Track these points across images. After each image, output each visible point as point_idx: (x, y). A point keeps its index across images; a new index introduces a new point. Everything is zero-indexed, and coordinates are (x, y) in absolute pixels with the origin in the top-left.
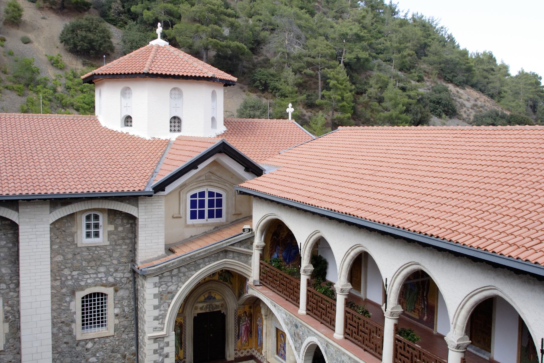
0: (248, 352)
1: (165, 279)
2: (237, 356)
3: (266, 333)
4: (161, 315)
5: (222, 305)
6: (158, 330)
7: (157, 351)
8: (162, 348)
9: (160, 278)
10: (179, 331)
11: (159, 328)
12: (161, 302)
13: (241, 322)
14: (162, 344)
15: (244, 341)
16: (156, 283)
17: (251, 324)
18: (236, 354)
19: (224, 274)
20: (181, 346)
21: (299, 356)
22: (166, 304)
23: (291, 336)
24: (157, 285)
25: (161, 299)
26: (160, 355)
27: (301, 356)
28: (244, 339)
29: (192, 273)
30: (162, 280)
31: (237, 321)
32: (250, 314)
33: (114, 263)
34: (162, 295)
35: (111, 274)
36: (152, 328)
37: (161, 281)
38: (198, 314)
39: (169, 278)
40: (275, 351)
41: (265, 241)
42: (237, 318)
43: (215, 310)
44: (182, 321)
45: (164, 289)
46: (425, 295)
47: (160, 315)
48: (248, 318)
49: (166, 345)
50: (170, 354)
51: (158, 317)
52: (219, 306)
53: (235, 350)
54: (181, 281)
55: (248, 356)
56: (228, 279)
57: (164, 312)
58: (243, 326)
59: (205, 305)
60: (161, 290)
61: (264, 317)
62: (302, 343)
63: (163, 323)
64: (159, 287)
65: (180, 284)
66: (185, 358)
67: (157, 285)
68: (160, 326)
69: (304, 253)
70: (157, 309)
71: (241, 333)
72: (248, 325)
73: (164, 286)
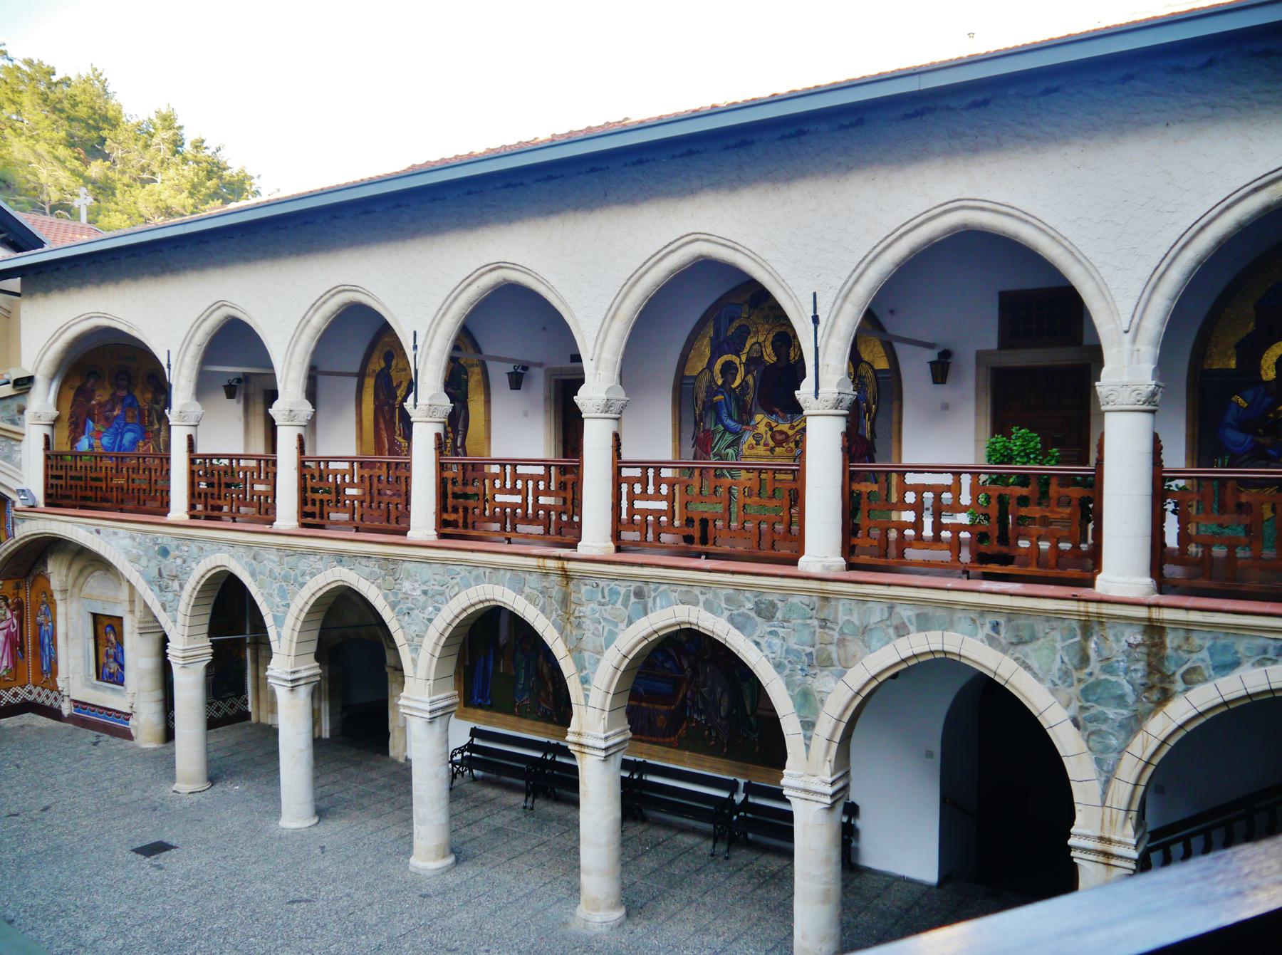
3: (67, 635)
21: (175, 621)
23: (149, 582)
27: (180, 618)
32: (18, 602)
40: (93, 671)
41: (58, 404)
46: (459, 444)
48: (12, 611)
55: (16, 705)
61: (57, 596)
62: (181, 587)
69: (179, 373)
72: (13, 630)
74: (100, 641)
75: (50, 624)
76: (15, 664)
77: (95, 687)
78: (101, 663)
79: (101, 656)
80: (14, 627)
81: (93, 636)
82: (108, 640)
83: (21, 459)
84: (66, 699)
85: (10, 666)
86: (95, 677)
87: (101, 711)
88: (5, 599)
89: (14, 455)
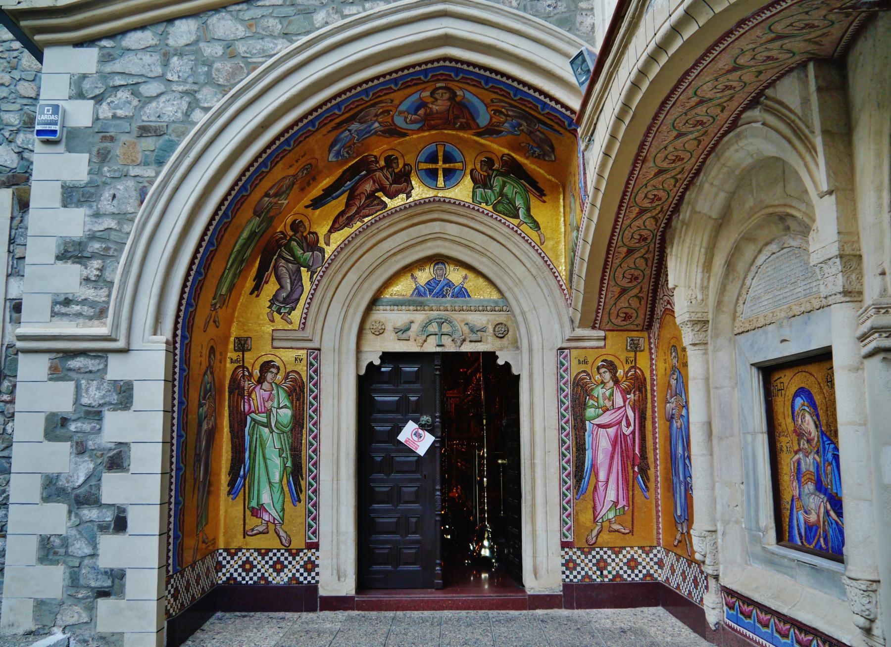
0: (632, 564)
1: (131, 64)
2: (576, 577)
3: (709, 424)
4: (100, 239)
5: (501, 331)
6: (79, 315)
7: (64, 421)
8: (95, 414)
9: (107, 58)
10: (286, 415)
11: (84, 302)
12: (99, 172)
13: (590, 412)
14: (93, 391)
15: (608, 505)
16: (84, 76)
17: (642, 426)
18: (569, 565)
19: (497, 182)
20: (297, 484)
22: (131, 183)
24: (87, 85)
25: (103, 157)
26: (81, 450)
28: (611, 495)
29: (268, 44)
30: (117, 66)
31: (568, 403)
32: (636, 377)
33: (23, 92)
34: (112, 139)
35: (7, 134)
36: (47, 301)
37: (109, 68)
38: (387, 357)
39: (147, 58)
42: (568, 390)
43: (467, 348)
44: (302, 368)
45: (120, 113)
47: (93, 237)
48: (625, 392)
49: (114, 398)
50: (135, 452)
51: (80, 245)
52: (483, 330)
53: (564, 545)
54: (210, 81)
55: (633, 585)
56: (519, 202)
57: (113, 224)
58: (601, 431)
59: (419, 317)
60: (105, 111)
61: (688, 337)
63: (100, 281)
64: (98, 99)
65: (206, 95)
66: (316, 546)
67: (87, 85)
68: (89, 293)
70: (79, 204)
71: (593, 466)
72: (627, 431)
73: (123, 95)
74: (783, 442)
75: (684, 412)
76: (631, 501)
77: (771, 561)
78: (787, 497)
79: (787, 477)
80: (628, 425)
81: (764, 427)
82: (800, 434)
83: (593, 25)
84: (712, 583)
85: (622, 503)
86: (772, 534)
87: (784, 627)
88: (611, 367)
89: (579, 19)
